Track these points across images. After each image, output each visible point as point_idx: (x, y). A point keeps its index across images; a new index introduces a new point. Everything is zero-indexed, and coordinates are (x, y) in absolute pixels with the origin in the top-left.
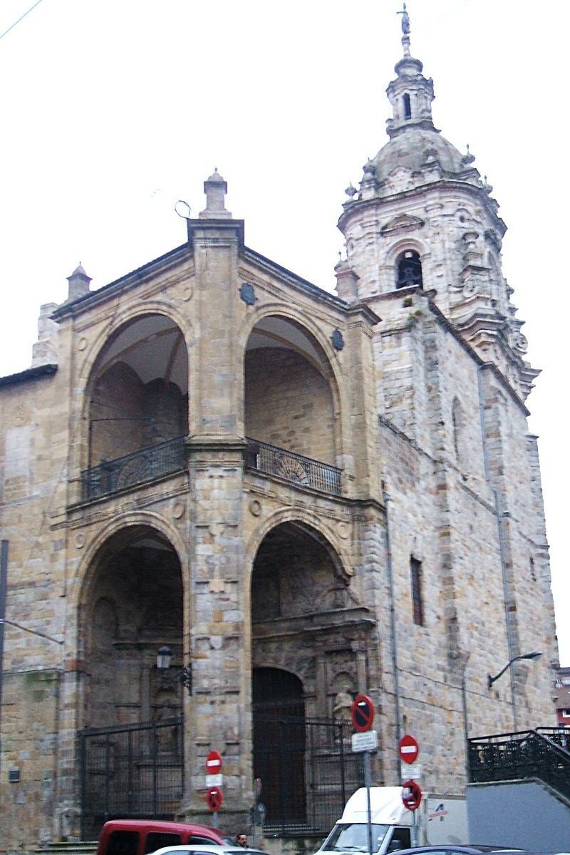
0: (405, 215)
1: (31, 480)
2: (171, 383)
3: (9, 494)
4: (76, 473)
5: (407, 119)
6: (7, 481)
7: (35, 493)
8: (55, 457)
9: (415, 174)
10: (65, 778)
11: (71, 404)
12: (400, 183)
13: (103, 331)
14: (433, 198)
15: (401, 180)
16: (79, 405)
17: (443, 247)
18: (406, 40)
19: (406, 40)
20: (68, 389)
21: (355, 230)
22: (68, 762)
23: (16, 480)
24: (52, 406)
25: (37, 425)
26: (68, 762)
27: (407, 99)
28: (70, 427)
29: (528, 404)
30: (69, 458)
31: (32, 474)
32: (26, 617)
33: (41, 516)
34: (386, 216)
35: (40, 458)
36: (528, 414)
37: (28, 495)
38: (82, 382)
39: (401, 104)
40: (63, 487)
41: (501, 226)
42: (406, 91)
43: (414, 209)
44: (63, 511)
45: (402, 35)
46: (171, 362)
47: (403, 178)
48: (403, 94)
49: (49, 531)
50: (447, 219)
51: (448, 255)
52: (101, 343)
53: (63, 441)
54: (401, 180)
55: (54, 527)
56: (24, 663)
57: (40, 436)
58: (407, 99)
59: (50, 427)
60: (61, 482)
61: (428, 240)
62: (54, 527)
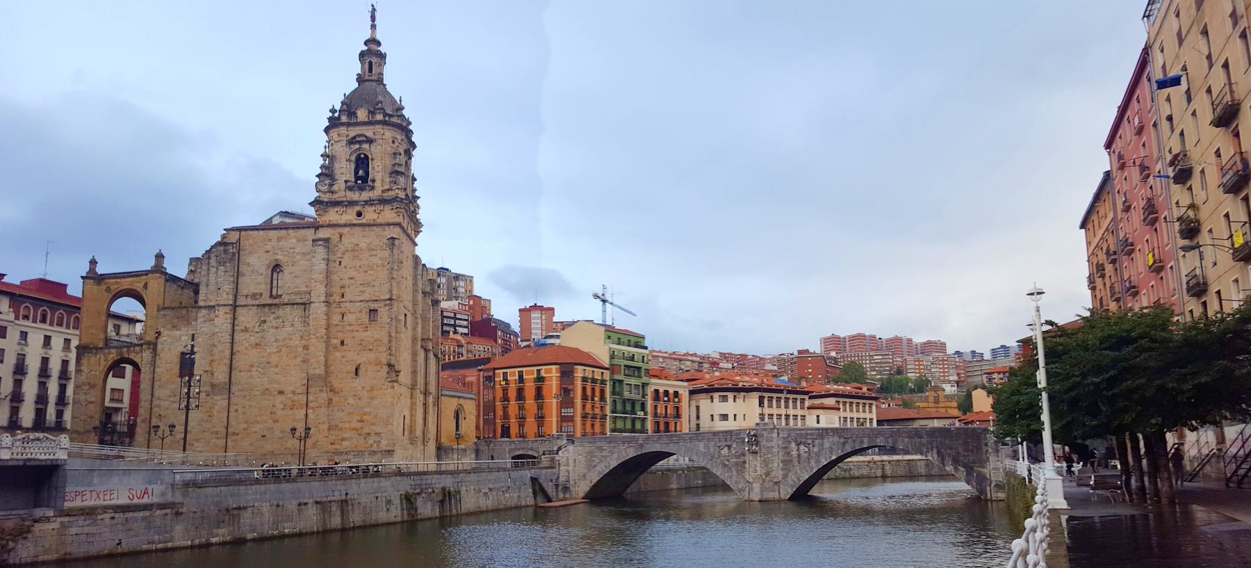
9: (372, 113)
18: (373, 27)
19: (373, 27)
21: (334, 133)
27: (370, 64)
29: (417, 240)
34: (353, 132)
36: (416, 245)
39: (367, 66)
41: (413, 146)
43: (368, 132)
45: (371, 23)
48: (368, 60)
58: (370, 64)
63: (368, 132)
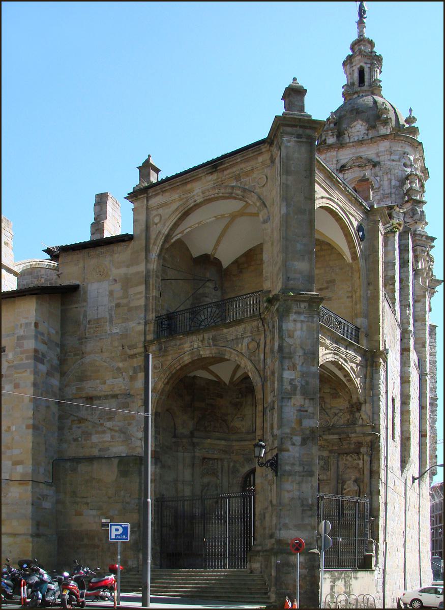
0: (361, 158)
1: (111, 321)
2: (216, 259)
3: (92, 331)
4: (152, 316)
5: (359, 86)
6: (89, 322)
7: (115, 331)
8: (132, 305)
11: (146, 265)
12: (358, 133)
13: (177, 210)
14: (384, 145)
15: (358, 131)
16: (153, 266)
17: (390, 183)
18: (361, 23)
19: (361, 23)
20: (143, 254)
23: (98, 320)
24: (128, 266)
25: (115, 281)
28: (147, 283)
30: (146, 306)
31: (111, 317)
33: (121, 348)
35: (118, 305)
37: (109, 332)
38: (155, 251)
39: (356, 75)
40: (141, 328)
42: (362, 64)
43: (368, 152)
44: (141, 345)
46: (218, 242)
47: (360, 130)
48: (358, 66)
49: (128, 359)
50: (394, 163)
51: (393, 191)
52: (174, 219)
53: (140, 293)
54: (358, 131)
55: (133, 356)
57: (117, 287)
59: (127, 282)
60: (139, 323)
61: (378, 178)
62: (133, 356)
63: (368, 152)
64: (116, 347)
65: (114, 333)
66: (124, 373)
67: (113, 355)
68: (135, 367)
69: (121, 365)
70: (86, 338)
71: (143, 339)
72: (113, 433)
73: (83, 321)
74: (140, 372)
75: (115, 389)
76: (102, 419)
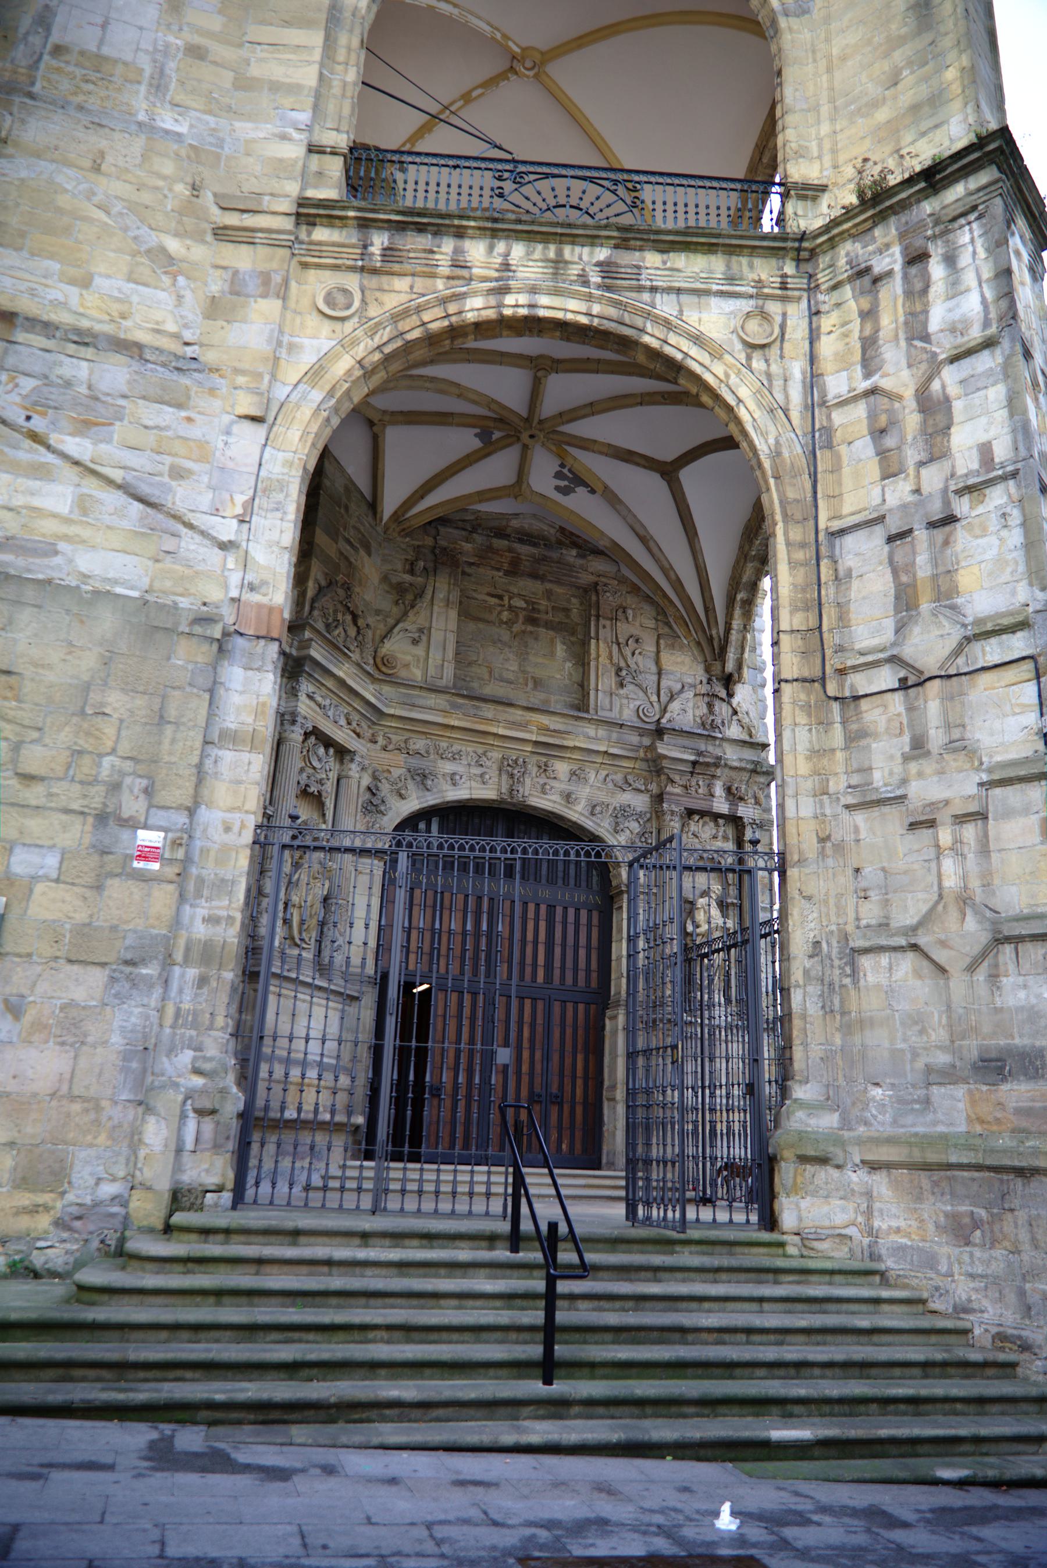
1: (158, 86)
6: (58, 50)
10: (192, 973)
22: (211, 920)
26: (211, 920)
32: (85, 426)
33: (181, 189)
37: (142, 117)
44: (287, 206)
49: (209, 238)
56: (58, 560)
60: (284, 137)
62: (242, 236)
64: (164, 178)
65: (167, 132)
66: (181, 280)
67: (146, 197)
68: (236, 273)
69: (173, 245)
70: (31, 96)
71: (293, 188)
72: (92, 487)
73: (27, 33)
74: (264, 296)
75: (127, 323)
76: (44, 414)
